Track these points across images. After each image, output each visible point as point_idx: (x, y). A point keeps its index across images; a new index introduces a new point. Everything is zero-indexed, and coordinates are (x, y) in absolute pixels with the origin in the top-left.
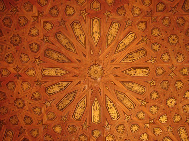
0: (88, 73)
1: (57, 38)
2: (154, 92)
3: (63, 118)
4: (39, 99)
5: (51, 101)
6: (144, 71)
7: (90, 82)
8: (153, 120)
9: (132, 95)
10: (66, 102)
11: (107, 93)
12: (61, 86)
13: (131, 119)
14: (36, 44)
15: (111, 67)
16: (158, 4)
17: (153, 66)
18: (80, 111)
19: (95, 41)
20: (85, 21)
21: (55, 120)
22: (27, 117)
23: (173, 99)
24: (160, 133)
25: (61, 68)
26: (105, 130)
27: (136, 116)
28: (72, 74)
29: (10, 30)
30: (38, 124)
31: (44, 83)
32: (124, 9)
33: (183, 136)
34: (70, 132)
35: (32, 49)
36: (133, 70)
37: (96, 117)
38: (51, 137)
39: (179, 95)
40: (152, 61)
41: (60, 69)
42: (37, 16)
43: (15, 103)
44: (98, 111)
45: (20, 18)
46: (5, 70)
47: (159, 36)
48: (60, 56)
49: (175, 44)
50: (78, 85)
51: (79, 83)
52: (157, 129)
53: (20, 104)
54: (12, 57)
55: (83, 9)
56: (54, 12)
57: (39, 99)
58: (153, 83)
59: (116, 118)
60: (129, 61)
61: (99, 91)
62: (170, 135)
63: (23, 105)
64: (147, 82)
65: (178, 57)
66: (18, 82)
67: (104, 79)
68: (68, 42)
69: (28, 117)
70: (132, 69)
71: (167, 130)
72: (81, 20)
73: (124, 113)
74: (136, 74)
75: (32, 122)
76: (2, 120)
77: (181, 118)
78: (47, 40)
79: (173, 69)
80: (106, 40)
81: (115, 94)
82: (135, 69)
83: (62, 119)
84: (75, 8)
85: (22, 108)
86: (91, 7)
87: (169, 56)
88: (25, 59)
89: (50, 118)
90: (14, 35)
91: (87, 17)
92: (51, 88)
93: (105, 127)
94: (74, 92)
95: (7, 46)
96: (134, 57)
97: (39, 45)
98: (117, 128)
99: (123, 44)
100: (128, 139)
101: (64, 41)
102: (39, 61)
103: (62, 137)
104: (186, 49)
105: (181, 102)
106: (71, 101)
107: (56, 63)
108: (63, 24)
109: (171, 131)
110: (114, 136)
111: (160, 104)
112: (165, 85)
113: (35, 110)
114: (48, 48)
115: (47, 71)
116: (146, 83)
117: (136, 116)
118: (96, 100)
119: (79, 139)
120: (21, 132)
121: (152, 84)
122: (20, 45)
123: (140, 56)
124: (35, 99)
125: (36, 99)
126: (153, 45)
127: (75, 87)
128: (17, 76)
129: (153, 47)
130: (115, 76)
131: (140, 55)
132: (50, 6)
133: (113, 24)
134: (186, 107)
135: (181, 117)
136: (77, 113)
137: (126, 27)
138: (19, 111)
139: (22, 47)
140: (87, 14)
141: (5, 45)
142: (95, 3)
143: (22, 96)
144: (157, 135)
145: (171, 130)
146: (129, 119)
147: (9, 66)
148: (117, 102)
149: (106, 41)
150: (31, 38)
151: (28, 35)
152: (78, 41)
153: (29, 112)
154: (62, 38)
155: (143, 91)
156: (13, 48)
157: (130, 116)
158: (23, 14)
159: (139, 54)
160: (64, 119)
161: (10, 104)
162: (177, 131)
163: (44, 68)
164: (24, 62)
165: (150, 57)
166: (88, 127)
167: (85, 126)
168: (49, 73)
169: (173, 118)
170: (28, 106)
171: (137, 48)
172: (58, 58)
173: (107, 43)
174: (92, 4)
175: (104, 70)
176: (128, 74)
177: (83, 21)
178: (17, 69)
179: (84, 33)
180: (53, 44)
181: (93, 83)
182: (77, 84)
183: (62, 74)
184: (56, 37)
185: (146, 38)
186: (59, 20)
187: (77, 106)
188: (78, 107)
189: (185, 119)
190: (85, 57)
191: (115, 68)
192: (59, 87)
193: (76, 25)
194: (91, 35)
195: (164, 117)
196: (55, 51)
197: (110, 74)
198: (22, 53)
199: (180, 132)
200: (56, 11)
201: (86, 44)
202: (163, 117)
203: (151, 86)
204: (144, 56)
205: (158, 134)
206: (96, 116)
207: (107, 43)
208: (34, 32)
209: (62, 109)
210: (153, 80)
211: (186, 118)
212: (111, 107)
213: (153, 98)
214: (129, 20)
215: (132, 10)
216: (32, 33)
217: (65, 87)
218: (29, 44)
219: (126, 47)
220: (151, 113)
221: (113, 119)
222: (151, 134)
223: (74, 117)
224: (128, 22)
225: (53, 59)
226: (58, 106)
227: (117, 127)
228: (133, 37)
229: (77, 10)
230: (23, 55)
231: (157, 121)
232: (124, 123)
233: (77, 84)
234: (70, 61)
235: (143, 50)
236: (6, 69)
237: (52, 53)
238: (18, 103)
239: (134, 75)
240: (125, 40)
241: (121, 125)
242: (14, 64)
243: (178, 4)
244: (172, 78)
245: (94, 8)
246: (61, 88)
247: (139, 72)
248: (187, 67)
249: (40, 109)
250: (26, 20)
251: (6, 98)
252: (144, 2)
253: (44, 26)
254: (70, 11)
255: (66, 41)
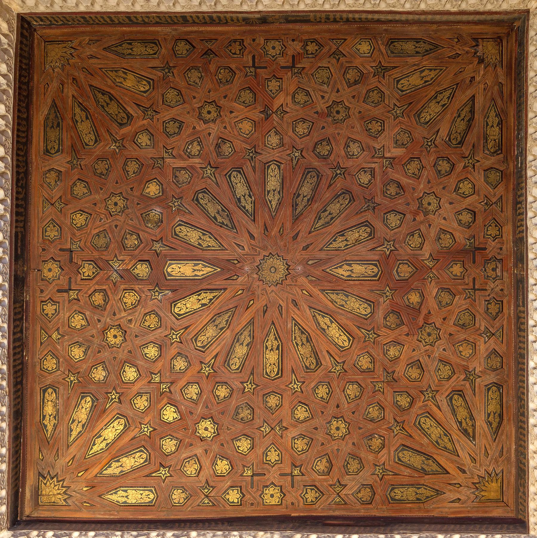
0: (271, 253)
1: (341, 194)
2: (230, 391)
3: (178, 202)
4: (219, 154)
5: (214, 179)
6: (275, 367)
7: (253, 258)
8: (168, 390)
9: (225, 344)
10: (212, 209)
11: (230, 292)
12: (245, 199)
13: (173, 343)
14: (331, 152)
15: (283, 301)
16: (410, 395)
17: (284, 387)
18: (193, 236)
19: (335, 268)
20: (373, 249)
21: (172, 184)
22: (180, 126)
23: (214, 433)
24: (139, 409)
25: (281, 201)
26: (151, 287)
27: (179, 354)
28: (269, 222)
29: (358, 102)
30: (165, 149)
31: (251, 165)
32: (398, 326)
33: (128, 461)
34: (146, 215)
35: (321, 143)
36: (275, 343)
37: (179, 270)
38: (134, 173)
39: (222, 445)
40: (295, 383)
41: (279, 198)
42: (385, 156)
43: (210, 102)
44: (193, 274)
45: (381, 123)
46: (279, 86)
47: (346, 396)
48: (306, 198)
49: (330, 432)
50: (248, 235)
51: (252, 237)
52: (147, 400)
53: (209, 112)
54: (305, 102)
55: (397, 246)
56: (392, 190)
57: (219, 154)
58: (248, 387)
59: (176, 310)
60: (295, 336)
61: (234, 276)
62: (133, 431)
63: (206, 120)
64: (252, 373)
65: (304, 439)
66: (254, 111)
67: (259, 287)
68: (334, 215)
69: (180, 128)
70: (278, 342)
71: (143, 424)
72: (377, 241)
73: (186, 328)
74: (268, 352)
75: (169, 135)
76: (173, 73)
77: (170, 455)
78: (337, 175)
79: (278, 428)
80: (336, 290)
81: (227, 308)
82: (278, 349)
83: (176, 199)
84: (400, 229)
85: (200, 117)
86: (401, 262)
87: (305, 421)
88: (301, 129)
89: (178, 174)
90: (350, 108)
91: (382, 252)
92: (242, 180)
93: (157, 288)
94: (232, 226)
95: (328, 93)
96: (302, 345)
97: (328, 158)
98: (154, 314)
99: (329, 323)
100: (126, 337)
101: (334, 208)
102: (296, 157)
103: (134, 196)
104: (320, 457)
105: (206, 451)
106: (215, 218)
107: (293, 190)
108: (367, 207)
109: (142, 433)
110: (135, 307)
111: (204, 403)
112: (245, 413)
113: (195, 143)
114: (322, 175)
115: (276, 173)
116: (249, 373)
117: (178, 353)
118: (216, 270)
119: (129, 233)
120: (147, 111)
121: (247, 385)
122: (330, 119)
123: (306, 359)
124: (218, 146)
125: (220, 147)
126: (326, 385)
127: (243, 228)
128: (267, 111)
129: (323, 385)
130: (265, 308)
131: (307, 358)
132: (404, 181)
133: (367, 304)
134: (196, 463)
135: (173, 453)
136: (188, 230)
137: (363, 330)
138: (194, 110)
139: (325, 124)
140: (388, 253)
141: (329, 90)
142: (410, 270)
143: (226, 119)
144: (133, 401)
145: (144, 431)
146: (173, 339)
147: (287, 95)
148: (210, 313)
149: (334, 290)
150: (342, 142)
151: (349, 138)
152: (334, 236)
153: (190, 131)
154: (341, 205)
155: (233, 367)
156: (324, 107)
157: (178, 340)
158: (389, 127)
159: (308, 356)
160: (176, 204)
161: (209, 92)
162: (141, 447)
163: (282, 166)
164: (296, 127)
165: (302, 380)
166: (158, 251)
167: (160, 247)
168: (271, 176)
169: (171, 436)
170: (203, 130)
171: (321, 351)
172: (302, 196)
173: (331, 293)
174: (407, 264)
175: (277, 285)
176: (267, 335)
177: (375, 245)
178: (282, 113)
179: (349, 248)
180: (330, 185)
181: (251, 263)
182: (249, 232)
183: (270, 202)
184: (343, 193)
185: (341, 370)
186: (376, 198)
187: (205, 232)
188: (201, 232)
189: (168, 464)
190: (303, 249)
191: (280, 308)
192: (244, 196)
193: (367, 233)
194: (346, 260)
195: (175, 415)
196: (315, 190)
197: (269, 298)
198: (313, 123)
199: (138, 454)
200: (393, 194)
201: (328, 250)
202: (175, 412)
203: (242, 383)
204: (305, 365)
205: (135, 404)
206: (181, 270)
207: (331, 293)
208: (354, 148)
209: (197, 200)
210: (254, 386)
211: (171, 466)
212: (200, 300)
213: (217, 389)
214: (375, 336)
215: (397, 343)
216: (351, 144)
217: (244, 207)
218: (330, 138)
219: (322, 331)
220: (185, 386)
221: (175, 305)
222: (136, 388)
223: (180, 225)
224: (371, 334)
225: (300, 186)
226: (205, 191)
227: (157, 313)
228: (343, 343)
229: (396, 233)
230: (309, 126)
231: (165, 401)
232: (164, 328)
233: (249, 232)
234: (296, 219)
235: (317, 364)
236: (280, 89)
237: (311, 184)
238: (211, 110)
239: (267, 348)
240: (337, 328)
241: (161, 321)
242: (291, 105)
243: (411, 436)
244: (259, 429)
245: (398, 267)
246: (242, 199)
247: (272, 357)
248: (281, 461)
249: (198, 155)
250: (377, 134)
251: (221, 85)
252: (412, 367)
253: (365, 169)
254: (393, 220)
255: (335, 211)
